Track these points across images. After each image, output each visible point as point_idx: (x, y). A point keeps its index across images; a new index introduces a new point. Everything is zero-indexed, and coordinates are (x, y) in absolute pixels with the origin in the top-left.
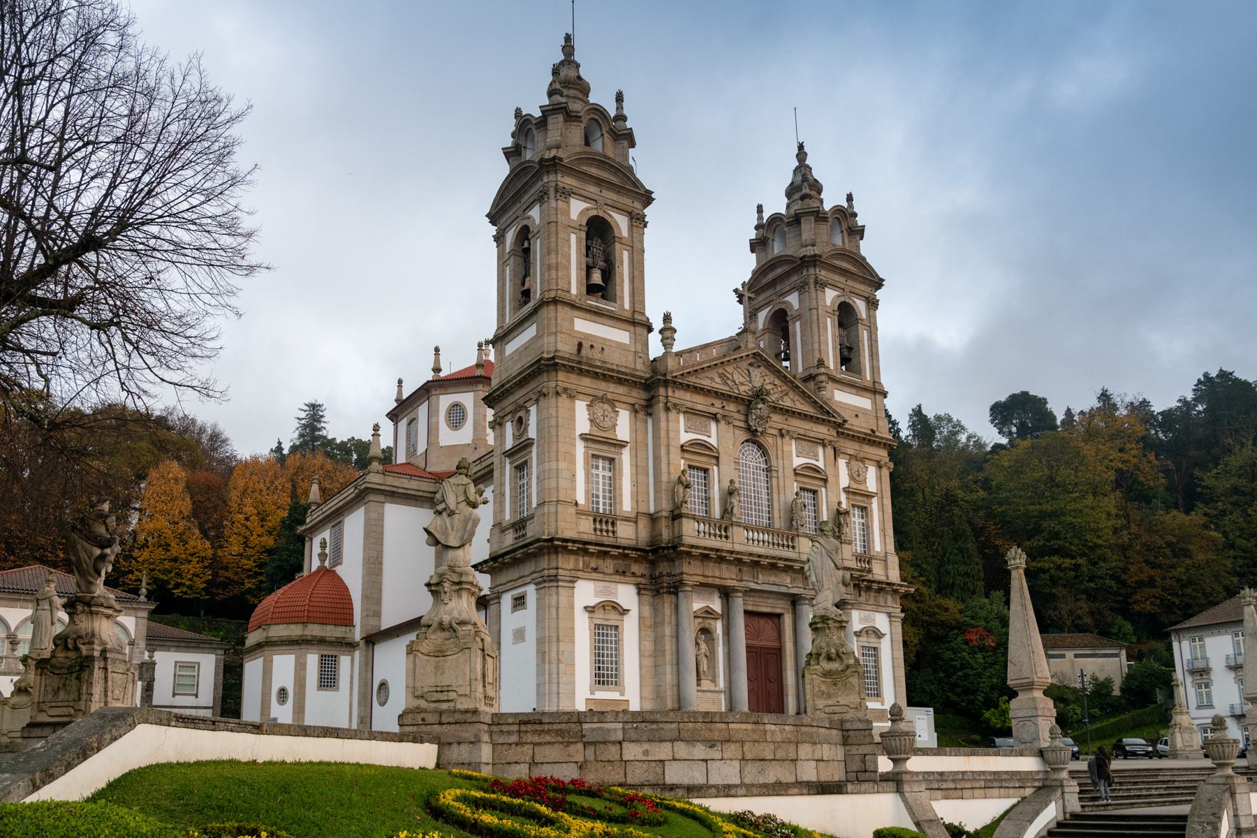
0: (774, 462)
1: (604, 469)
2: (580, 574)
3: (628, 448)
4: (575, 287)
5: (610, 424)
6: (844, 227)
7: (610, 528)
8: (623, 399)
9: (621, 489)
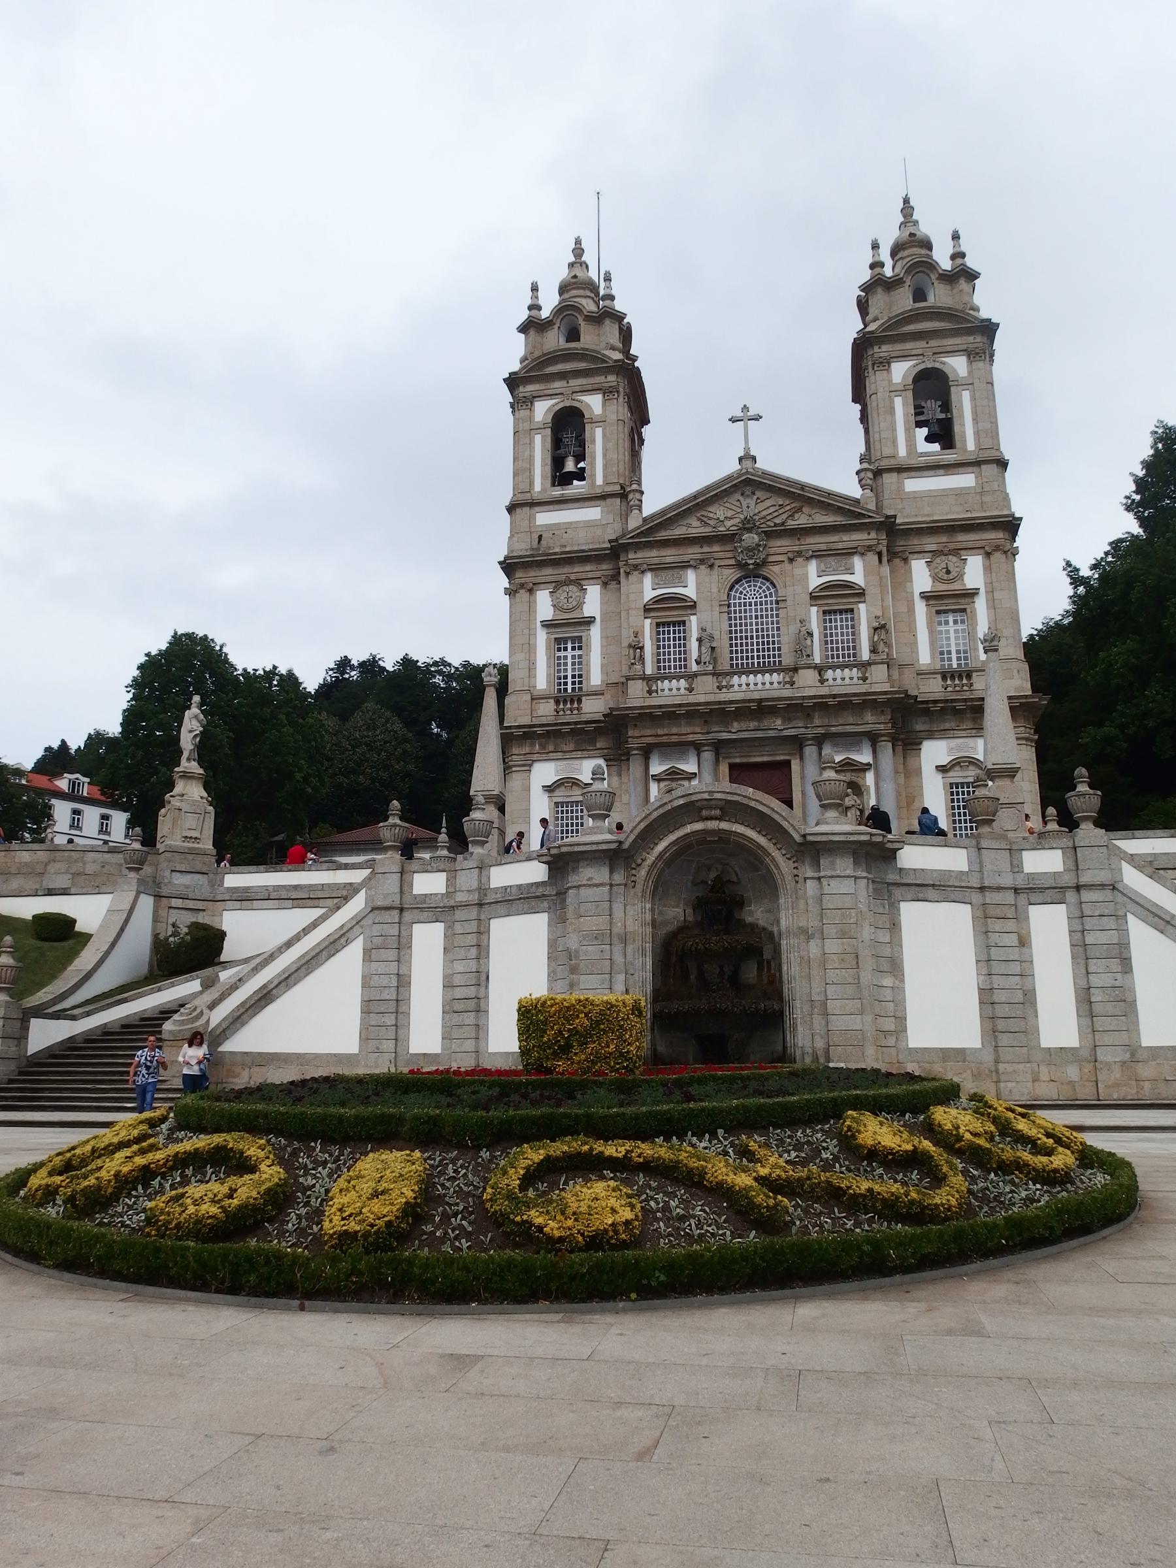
1: (573, 649)
2: (535, 757)
5: (575, 603)
6: (934, 277)
7: (576, 705)
8: (590, 575)
9: (588, 665)
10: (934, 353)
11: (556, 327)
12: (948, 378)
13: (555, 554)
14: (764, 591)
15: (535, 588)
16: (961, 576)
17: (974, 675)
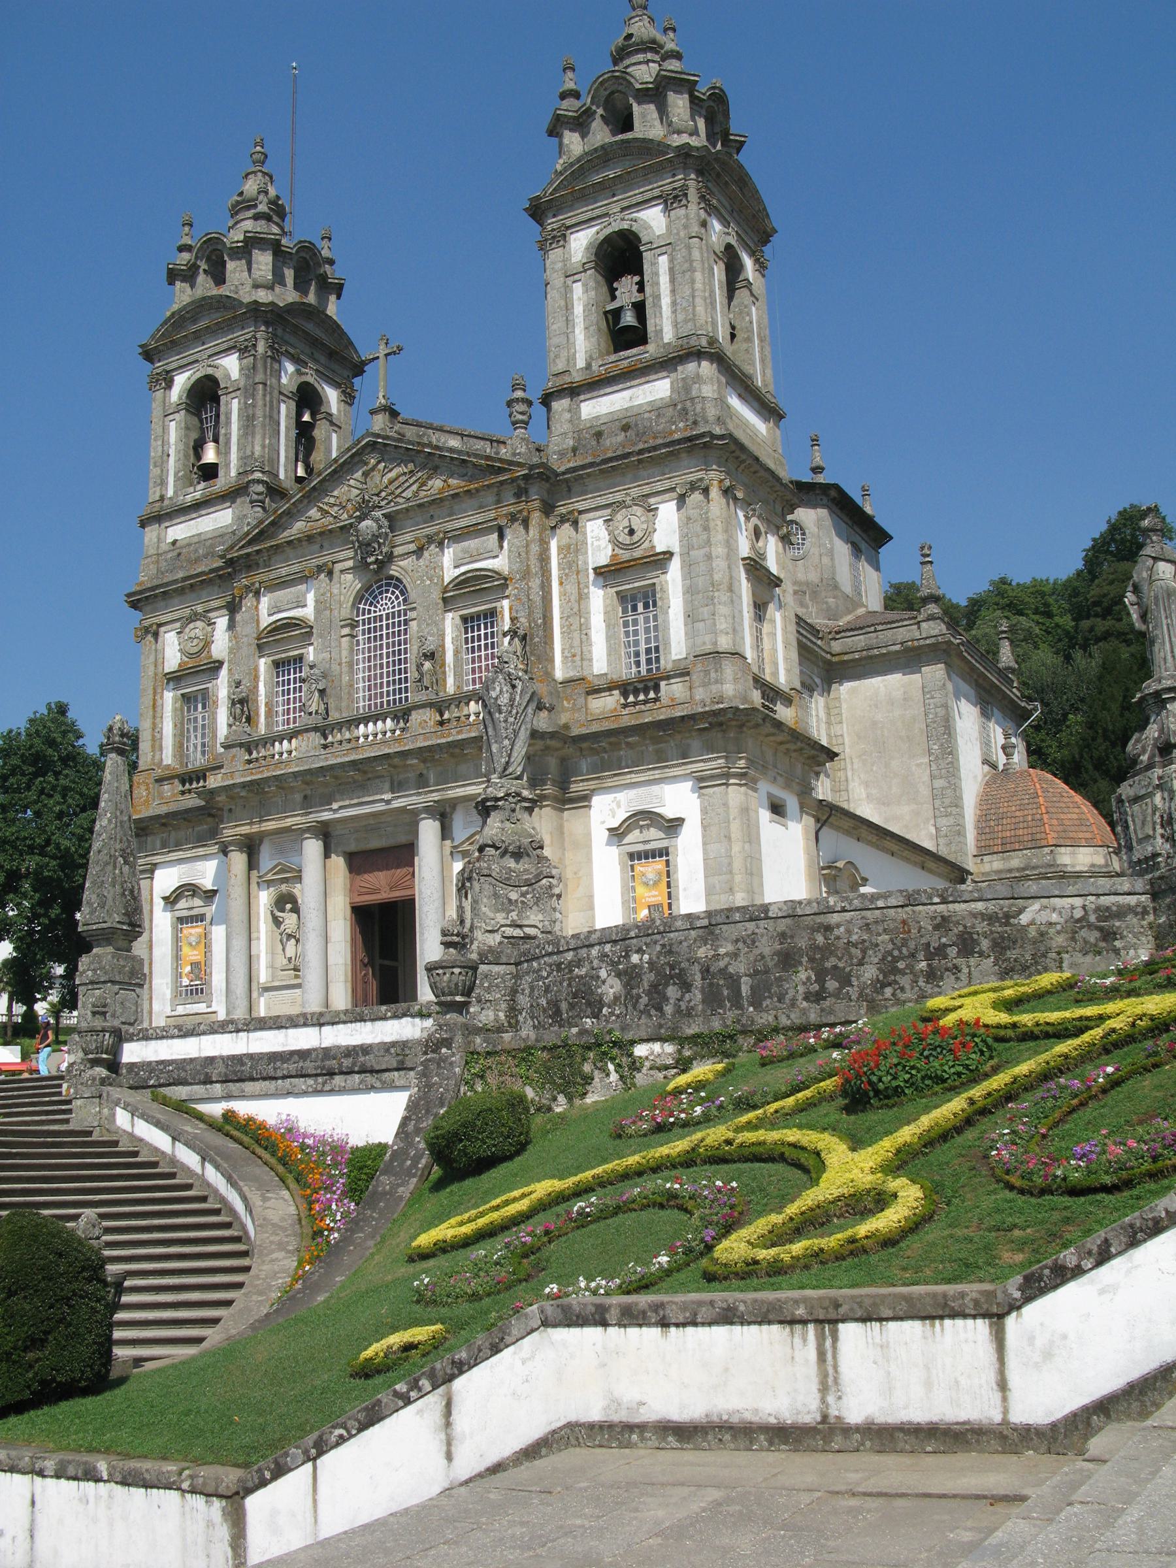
3: (225, 666)
5: (201, 645)
10: (623, 209)
11: (201, 271)
12: (639, 240)
13: (175, 581)
14: (397, 598)
15: (162, 629)
16: (650, 532)
17: (663, 684)
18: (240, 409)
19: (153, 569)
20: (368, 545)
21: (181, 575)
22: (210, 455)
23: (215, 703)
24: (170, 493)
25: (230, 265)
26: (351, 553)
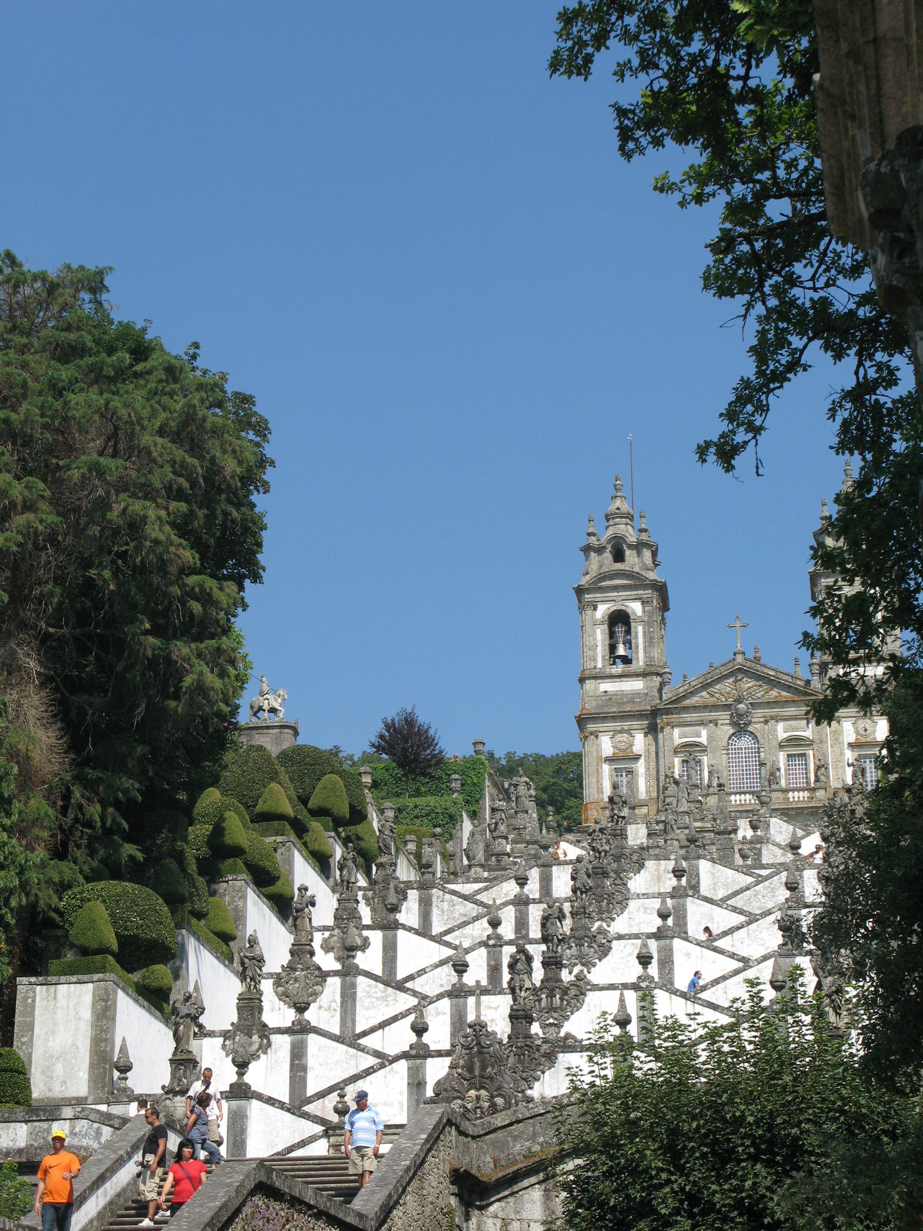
0: (761, 741)
4: (600, 662)
11: (608, 550)
13: (614, 712)
15: (600, 734)
18: (644, 632)
19: (594, 704)
20: (742, 715)
21: (614, 709)
22: (621, 651)
23: (637, 775)
24: (600, 665)
25: (628, 553)
26: (728, 717)
